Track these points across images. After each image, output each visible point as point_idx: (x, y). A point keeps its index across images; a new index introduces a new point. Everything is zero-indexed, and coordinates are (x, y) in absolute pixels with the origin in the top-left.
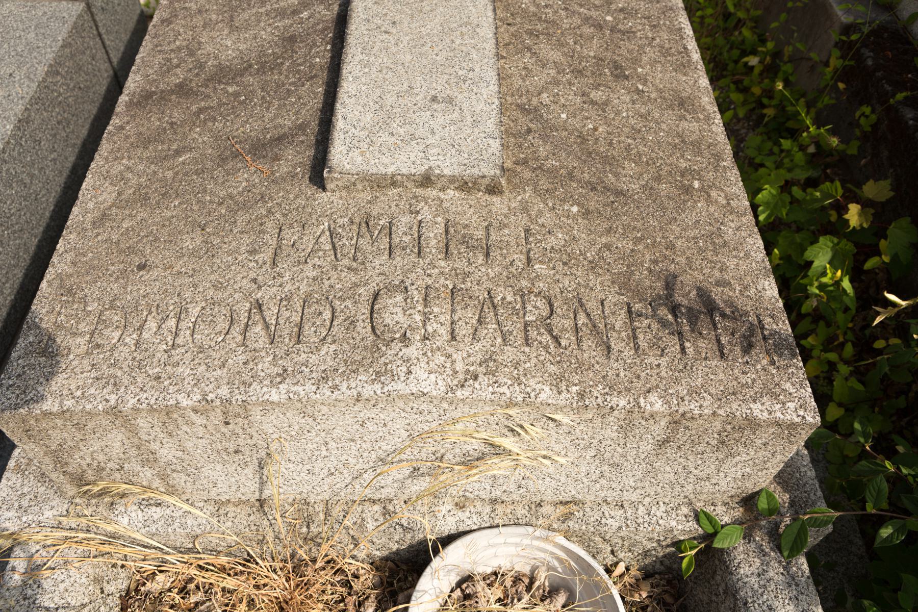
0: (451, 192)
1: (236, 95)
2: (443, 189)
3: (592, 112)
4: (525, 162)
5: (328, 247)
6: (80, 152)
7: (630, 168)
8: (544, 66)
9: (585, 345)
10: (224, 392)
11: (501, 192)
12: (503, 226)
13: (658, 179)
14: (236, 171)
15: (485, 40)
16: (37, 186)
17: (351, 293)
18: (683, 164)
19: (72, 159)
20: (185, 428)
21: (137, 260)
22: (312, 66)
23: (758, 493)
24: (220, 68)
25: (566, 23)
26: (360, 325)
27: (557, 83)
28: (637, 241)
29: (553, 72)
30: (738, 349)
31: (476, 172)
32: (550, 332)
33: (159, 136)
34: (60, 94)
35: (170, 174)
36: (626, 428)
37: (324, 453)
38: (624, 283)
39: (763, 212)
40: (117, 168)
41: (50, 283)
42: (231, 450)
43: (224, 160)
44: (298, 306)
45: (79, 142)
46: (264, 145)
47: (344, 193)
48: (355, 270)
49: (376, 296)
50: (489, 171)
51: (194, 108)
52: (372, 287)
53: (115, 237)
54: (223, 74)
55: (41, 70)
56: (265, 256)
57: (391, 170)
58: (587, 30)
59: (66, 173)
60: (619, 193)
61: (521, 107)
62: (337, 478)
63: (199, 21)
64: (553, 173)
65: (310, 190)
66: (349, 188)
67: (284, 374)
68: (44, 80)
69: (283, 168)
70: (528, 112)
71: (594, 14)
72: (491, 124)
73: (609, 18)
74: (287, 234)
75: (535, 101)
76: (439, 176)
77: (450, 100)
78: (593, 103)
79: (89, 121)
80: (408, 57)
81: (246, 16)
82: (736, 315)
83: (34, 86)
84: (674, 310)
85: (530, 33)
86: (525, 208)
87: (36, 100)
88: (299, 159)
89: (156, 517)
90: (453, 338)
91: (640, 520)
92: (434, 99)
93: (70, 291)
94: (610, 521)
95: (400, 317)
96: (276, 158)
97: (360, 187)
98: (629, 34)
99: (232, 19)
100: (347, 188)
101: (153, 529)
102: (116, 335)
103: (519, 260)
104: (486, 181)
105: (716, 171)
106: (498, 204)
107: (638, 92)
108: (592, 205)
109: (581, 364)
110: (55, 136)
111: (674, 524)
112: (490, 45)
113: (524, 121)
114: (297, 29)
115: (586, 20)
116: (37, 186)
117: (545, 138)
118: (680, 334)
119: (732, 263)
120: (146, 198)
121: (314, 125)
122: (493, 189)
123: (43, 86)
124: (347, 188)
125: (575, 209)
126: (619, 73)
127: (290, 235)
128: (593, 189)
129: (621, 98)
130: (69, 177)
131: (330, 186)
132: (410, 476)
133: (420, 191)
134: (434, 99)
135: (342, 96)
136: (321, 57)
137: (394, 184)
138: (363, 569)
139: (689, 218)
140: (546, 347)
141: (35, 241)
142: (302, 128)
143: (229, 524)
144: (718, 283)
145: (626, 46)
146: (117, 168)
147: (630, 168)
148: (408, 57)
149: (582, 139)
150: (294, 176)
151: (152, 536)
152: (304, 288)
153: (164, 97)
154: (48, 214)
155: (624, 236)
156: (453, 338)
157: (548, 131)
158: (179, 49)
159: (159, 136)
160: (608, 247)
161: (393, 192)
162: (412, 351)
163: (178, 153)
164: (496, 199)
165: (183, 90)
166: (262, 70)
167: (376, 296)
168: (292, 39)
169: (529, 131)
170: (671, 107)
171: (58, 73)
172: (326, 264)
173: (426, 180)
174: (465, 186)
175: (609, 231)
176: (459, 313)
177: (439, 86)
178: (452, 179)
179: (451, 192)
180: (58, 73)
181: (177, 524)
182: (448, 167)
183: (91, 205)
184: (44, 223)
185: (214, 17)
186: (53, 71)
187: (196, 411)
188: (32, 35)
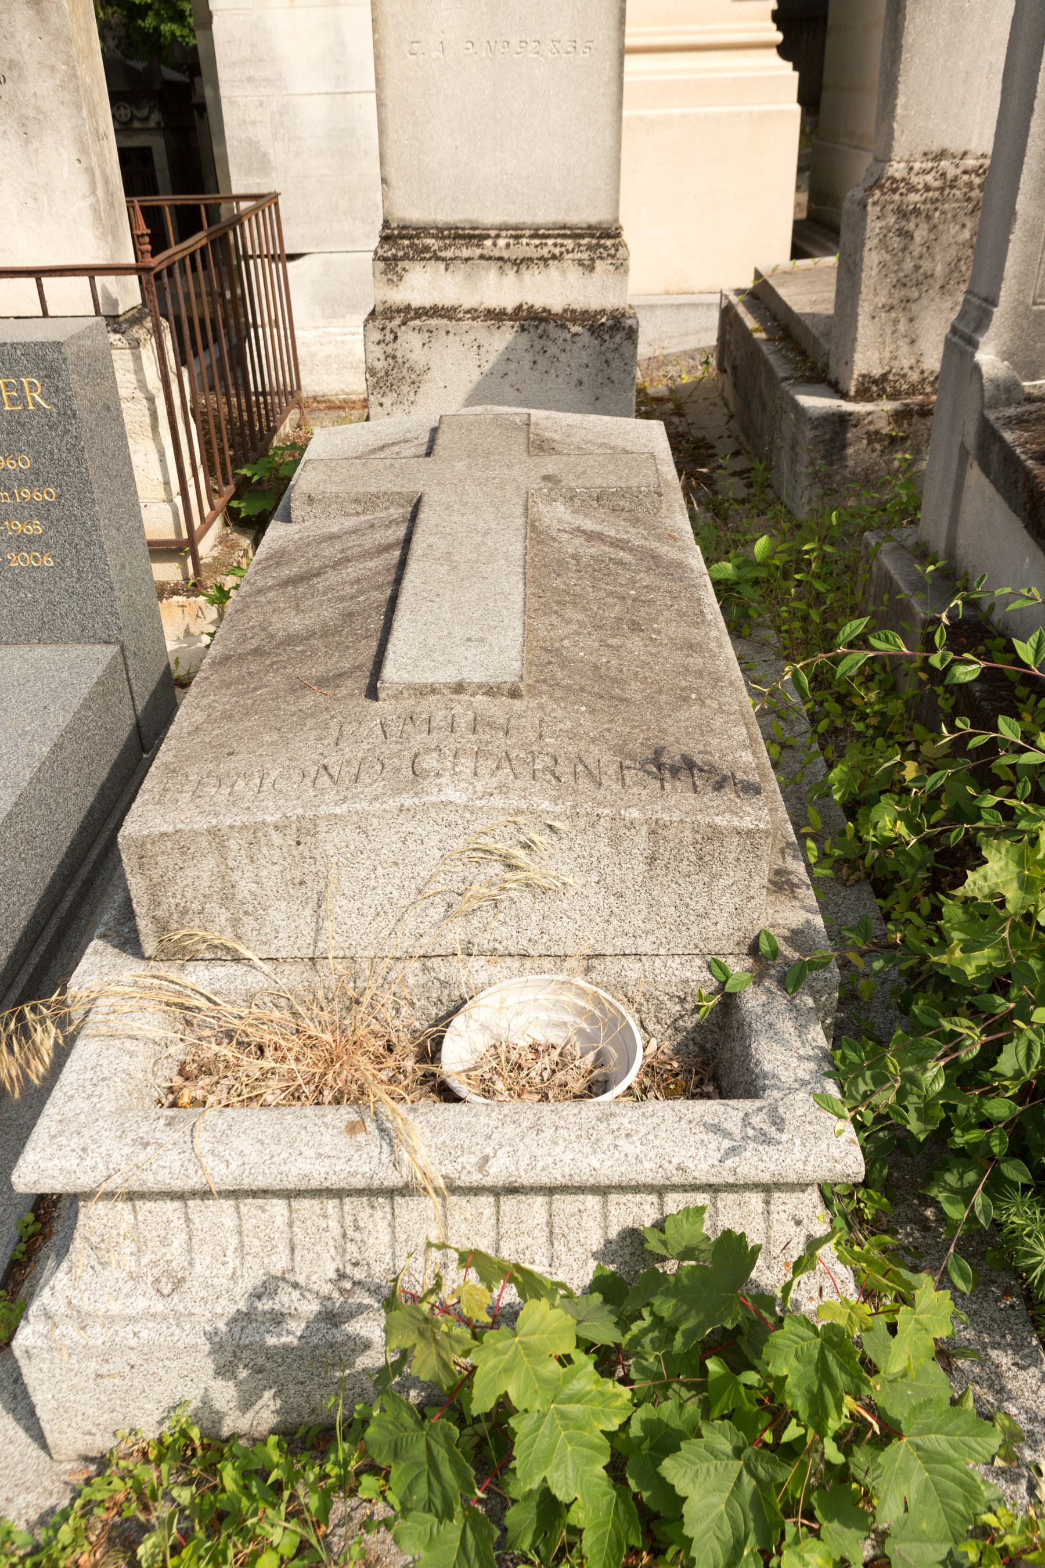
0: (479, 697)
1: (303, 652)
2: (473, 695)
3: (608, 652)
4: (544, 681)
5: (380, 732)
6: (99, 794)
7: (635, 685)
8: (568, 623)
9: (580, 781)
10: (300, 811)
11: (521, 696)
12: (520, 717)
13: (660, 692)
14: (304, 696)
15: (514, 602)
16: (59, 816)
17: (398, 755)
18: (684, 684)
19: (91, 799)
20: (265, 850)
21: (227, 751)
22: (367, 630)
23: (758, 937)
24: (289, 636)
25: (592, 596)
26: (403, 771)
27: (578, 634)
28: (634, 727)
29: (575, 627)
30: (709, 789)
31: (500, 680)
32: (554, 775)
33: (240, 680)
34: (89, 730)
35: (250, 702)
36: (615, 841)
37: (373, 883)
38: (619, 750)
39: (838, 791)
40: (205, 702)
41: (157, 768)
42: (296, 881)
43: (295, 691)
44: (356, 764)
45: (99, 784)
46: (327, 680)
47: (393, 701)
48: (401, 743)
49: (416, 756)
50: (510, 678)
51: (268, 662)
52: (414, 750)
53: (207, 740)
54: (291, 640)
55: (76, 704)
56: (331, 740)
57: (431, 681)
58: (610, 600)
59: (84, 812)
60: (622, 700)
61: (546, 649)
62: (381, 921)
63: (270, 609)
64: (568, 688)
65: (367, 702)
66: (397, 696)
67: (345, 800)
68: (79, 712)
69: (344, 691)
70: (551, 651)
71: (618, 589)
72: (515, 653)
73: (633, 592)
74: (346, 727)
75: (557, 645)
76: (469, 684)
77: (482, 640)
78: (609, 646)
79: (110, 764)
80: (449, 615)
81: (310, 603)
82: (713, 769)
83: (69, 716)
84: (660, 767)
85: (558, 603)
86: (541, 707)
87: (70, 729)
88: (357, 685)
89: (220, 975)
90: (475, 774)
91: (657, 972)
92: (469, 640)
93: (174, 771)
94: (629, 973)
95: (435, 764)
96: (338, 686)
97: (406, 695)
98: (650, 602)
99: (298, 605)
100: (395, 696)
101: (217, 986)
102: (214, 790)
103: (532, 736)
104: (508, 686)
105: (713, 688)
106: (518, 704)
107: (651, 639)
108: (598, 707)
109: (575, 791)
110: (80, 769)
111: (689, 974)
112: (519, 606)
113: (545, 657)
114: (354, 607)
115: (611, 594)
116: (59, 816)
117: (563, 667)
118: (662, 780)
119: (715, 742)
120: (231, 716)
121: (370, 665)
122: (514, 694)
123: (77, 717)
124: (395, 696)
125: (583, 709)
126: (635, 627)
127: (348, 729)
128: (601, 697)
129: (636, 644)
130: (86, 817)
131: (382, 695)
132: (446, 917)
133: (455, 697)
134: (469, 640)
135: (390, 647)
136: (376, 622)
137: (433, 691)
138: (405, 1037)
139: (681, 715)
140: (549, 782)
141: (50, 873)
142: (359, 667)
143: (285, 980)
144: (700, 752)
145: (644, 611)
146: (205, 702)
147: (635, 685)
148: (449, 615)
149: (596, 667)
150: (352, 695)
151: (216, 994)
152: (360, 755)
153: (241, 657)
154: (64, 849)
155: (624, 724)
156: (475, 774)
157: (565, 663)
158: (253, 627)
159: (240, 680)
160: (609, 730)
161: (433, 698)
162: (443, 780)
163: (255, 689)
164: (516, 701)
165: (257, 652)
166: (325, 634)
167: (416, 756)
168: (351, 615)
169: (550, 663)
170: (681, 649)
171: (90, 708)
172: (378, 742)
173: (459, 688)
174: (491, 691)
175: (611, 721)
176: (481, 762)
177: (474, 632)
178: (480, 686)
179: (479, 697)
180: (90, 708)
181: (238, 981)
182: (477, 677)
183: (185, 724)
184: (60, 856)
185: (282, 605)
186: (86, 706)
187: (276, 828)
188: (66, 674)
